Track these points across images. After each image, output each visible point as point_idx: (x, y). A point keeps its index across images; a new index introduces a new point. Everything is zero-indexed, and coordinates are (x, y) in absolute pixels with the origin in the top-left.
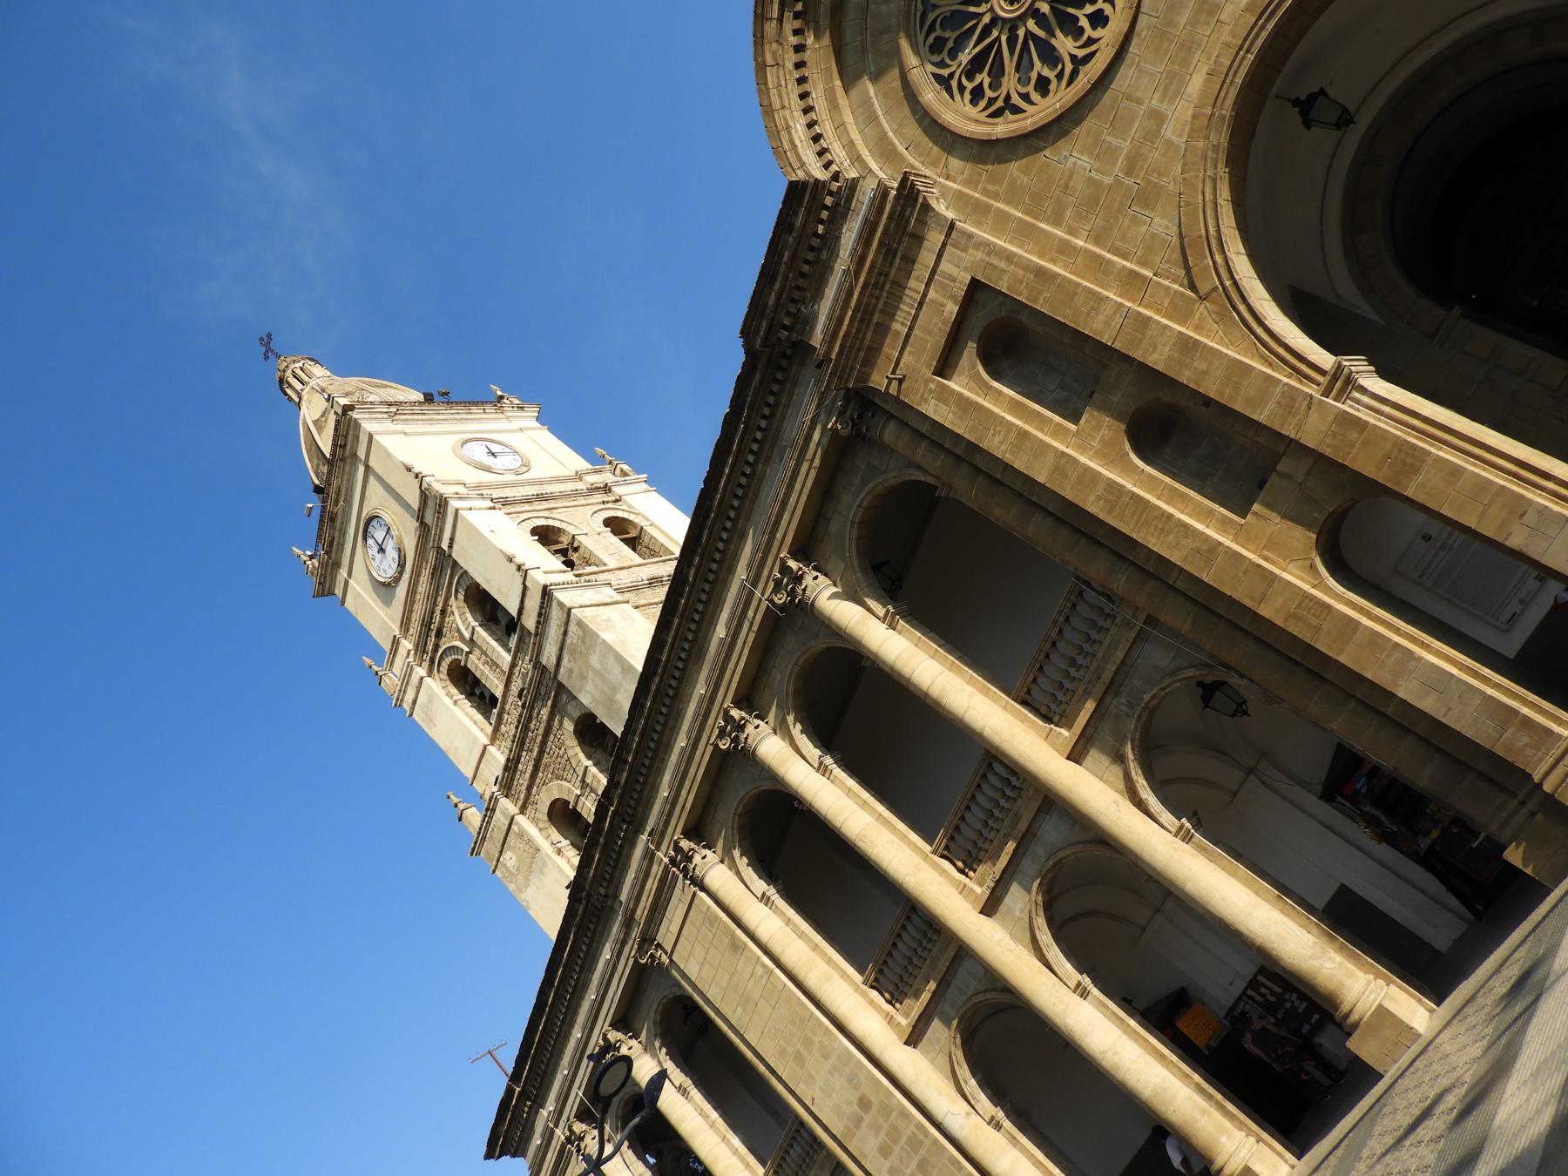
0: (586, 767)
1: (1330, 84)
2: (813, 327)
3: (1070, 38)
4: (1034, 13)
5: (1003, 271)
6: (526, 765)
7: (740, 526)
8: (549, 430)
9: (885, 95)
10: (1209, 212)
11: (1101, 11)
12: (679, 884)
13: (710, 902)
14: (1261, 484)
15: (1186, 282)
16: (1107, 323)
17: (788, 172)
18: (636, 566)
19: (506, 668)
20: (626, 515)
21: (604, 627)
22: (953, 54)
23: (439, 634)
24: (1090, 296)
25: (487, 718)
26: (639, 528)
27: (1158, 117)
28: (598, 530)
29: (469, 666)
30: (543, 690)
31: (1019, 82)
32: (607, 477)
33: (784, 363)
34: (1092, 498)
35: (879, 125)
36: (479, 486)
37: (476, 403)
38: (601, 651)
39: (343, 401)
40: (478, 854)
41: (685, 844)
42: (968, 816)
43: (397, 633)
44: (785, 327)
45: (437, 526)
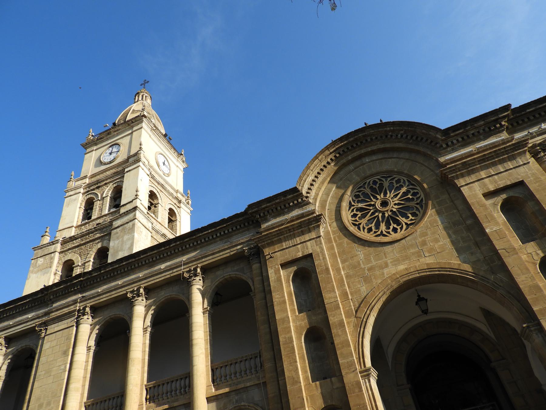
0: (90, 261)
1: (430, 300)
2: (266, 222)
3: (385, 227)
4: (383, 214)
5: (320, 259)
6: (76, 243)
7: (197, 247)
8: (184, 174)
9: (336, 193)
11: (397, 229)
12: (73, 319)
14: (325, 378)
15: (356, 309)
16: (330, 298)
17: (298, 185)
19: (103, 214)
20: (177, 213)
21: (138, 232)
22: (358, 202)
23: (98, 188)
24: (332, 287)
25: (83, 220)
26: (175, 219)
27: (387, 265)
28: (166, 209)
29: (95, 203)
30: (105, 230)
31: (366, 223)
32: (183, 199)
33: (251, 223)
34: (283, 336)
35: (328, 198)
36: (151, 167)
37: (175, 149)
38: (130, 237)
39: (145, 114)
40: (35, 250)
41: (88, 309)
42: (165, 385)
43: (89, 175)
44: (260, 215)
45: (130, 164)
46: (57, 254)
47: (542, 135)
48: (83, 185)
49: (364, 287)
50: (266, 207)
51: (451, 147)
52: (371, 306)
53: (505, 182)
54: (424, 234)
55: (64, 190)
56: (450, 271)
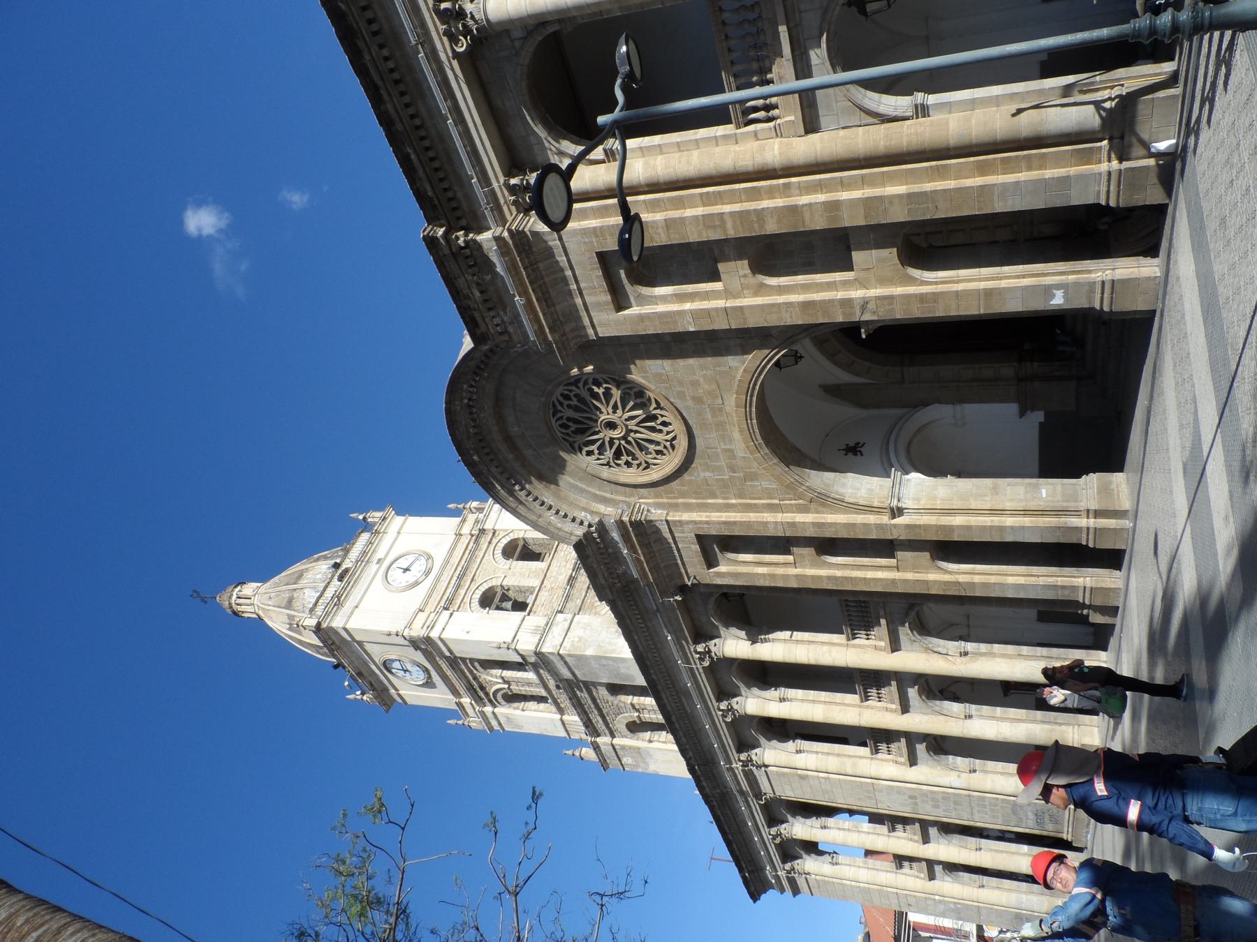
4: (631, 431)
9: (580, 479)
13: (775, 769)
16: (775, 528)
18: (547, 572)
19: (537, 681)
20: (508, 539)
21: (583, 646)
23: (482, 688)
28: (507, 567)
29: (515, 692)
31: (646, 454)
36: (426, 603)
39: (312, 622)
46: (616, 741)
48: (477, 710)
50: (604, 576)
51: (505, 327)
52: (796, 483)
53: (597, 277)
54: (681, 396)
55: (489, 732)
56: (755, 384)
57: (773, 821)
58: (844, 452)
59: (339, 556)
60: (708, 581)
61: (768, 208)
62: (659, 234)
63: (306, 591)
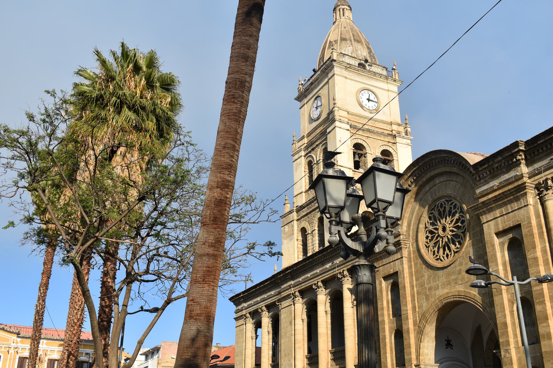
0: (315, 230)
4: (443, 239)
5: (401, 277)
9: (418, 213)
10: (430, 314)
13: (293, 309)
16: (405, 310)
20: (392, 152)
23: (313, 149)
27: (438, 288)
31: (433, 246)
36: (352, 114)
39: (335, 58)
40: (282, 218)
43: (305, 135)
45: (329, 124)
47: (549, 170)
49: (425, 304)
51: (483, 179)
54: (461, 264)
56: (469, 300)
57: (269, 307)
58: (447, 339)
59: (372, 60)
60: (377, 277)
61: (546, 306)
62: (531, 254)
63: (351, 47)
